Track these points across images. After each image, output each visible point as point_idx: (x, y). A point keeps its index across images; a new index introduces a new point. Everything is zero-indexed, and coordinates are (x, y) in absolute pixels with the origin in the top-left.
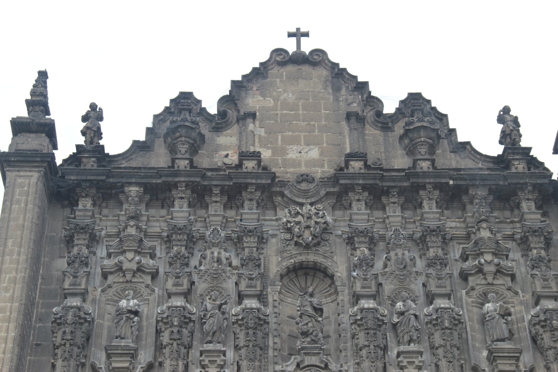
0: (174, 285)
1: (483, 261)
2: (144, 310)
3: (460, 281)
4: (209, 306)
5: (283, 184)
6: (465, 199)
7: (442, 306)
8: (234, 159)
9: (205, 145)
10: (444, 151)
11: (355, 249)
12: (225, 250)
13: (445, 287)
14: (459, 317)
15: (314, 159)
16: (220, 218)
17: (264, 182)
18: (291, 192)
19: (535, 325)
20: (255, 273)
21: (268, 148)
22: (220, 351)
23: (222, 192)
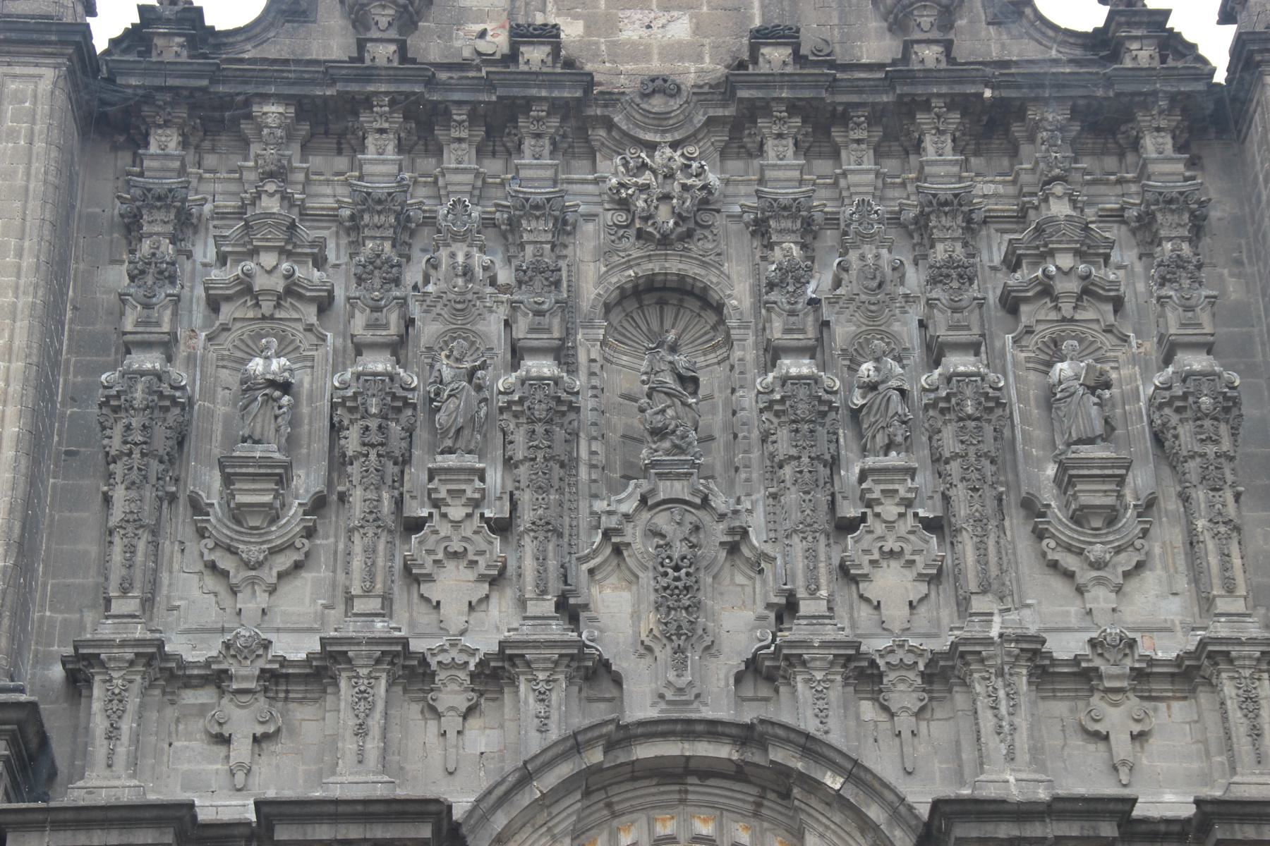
0: (369, 326)
1: (1052, 269)
2: (303, 379)
3: (1001, 314)
4: (447, 373)
5: (611, 99)
6: (1017, 130)
7: (961, 369)
8: (498, 41)
9: (434, 8)
10: (971, 22)
11: (770, 246)
12: (482, 249)
13: (968, 328)
14: (998, 394)
15: (680, 43)
16: (469, 178)
17: (566, 94)
18: (628, 118)
19: (1161, 407)
20: (548, 302)
21: (576, 17)
22: (473, 471)
23: (473, 118)
